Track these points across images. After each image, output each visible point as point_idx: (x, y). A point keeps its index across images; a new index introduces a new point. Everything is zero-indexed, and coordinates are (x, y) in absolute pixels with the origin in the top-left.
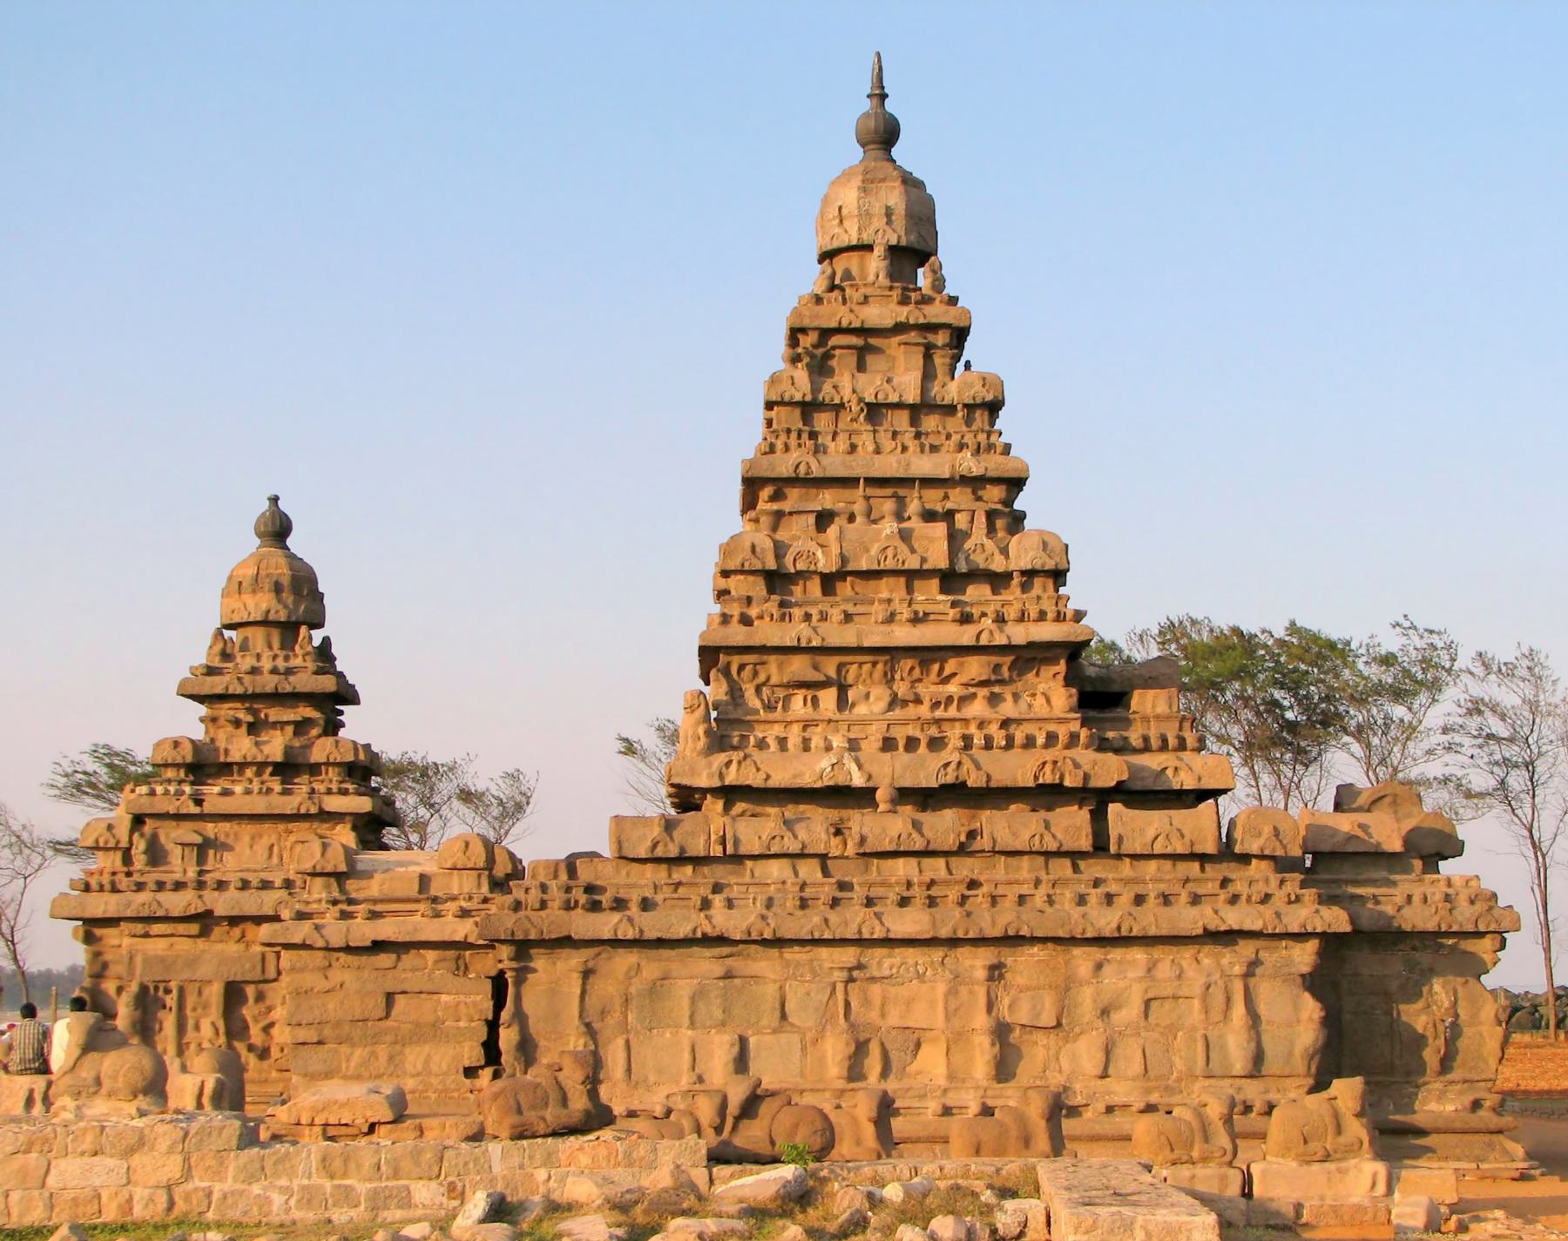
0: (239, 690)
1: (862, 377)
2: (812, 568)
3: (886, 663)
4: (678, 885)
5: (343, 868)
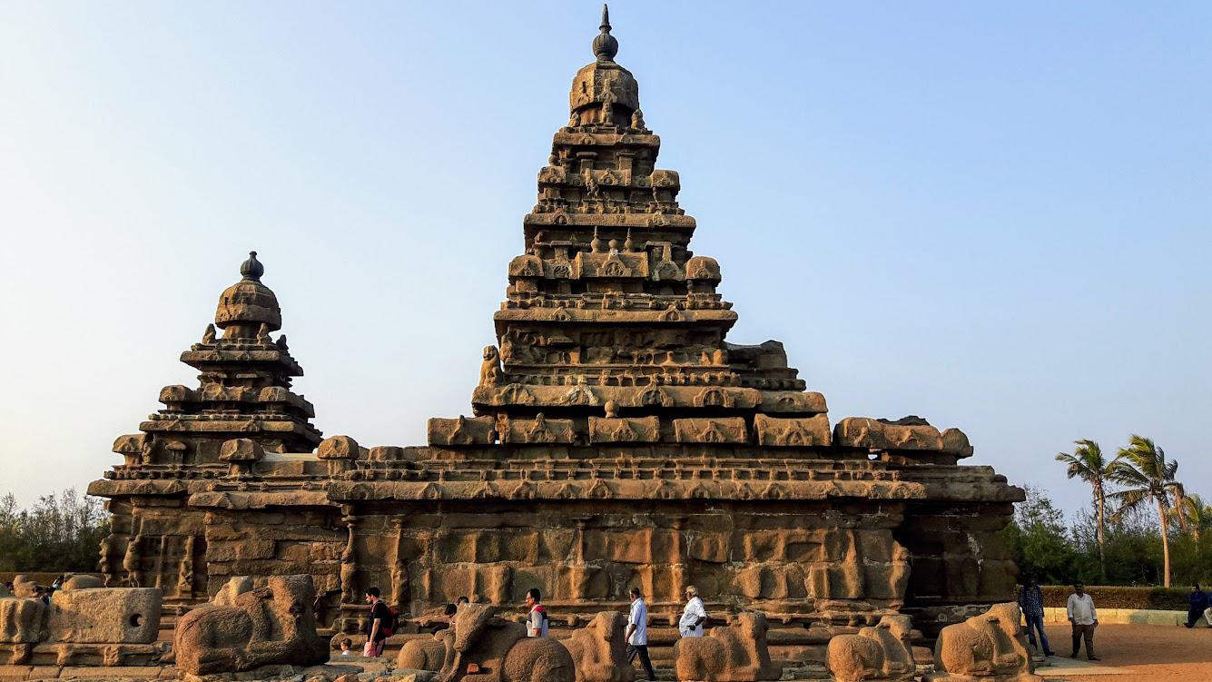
0: (219, 358)
2: (566, 276)
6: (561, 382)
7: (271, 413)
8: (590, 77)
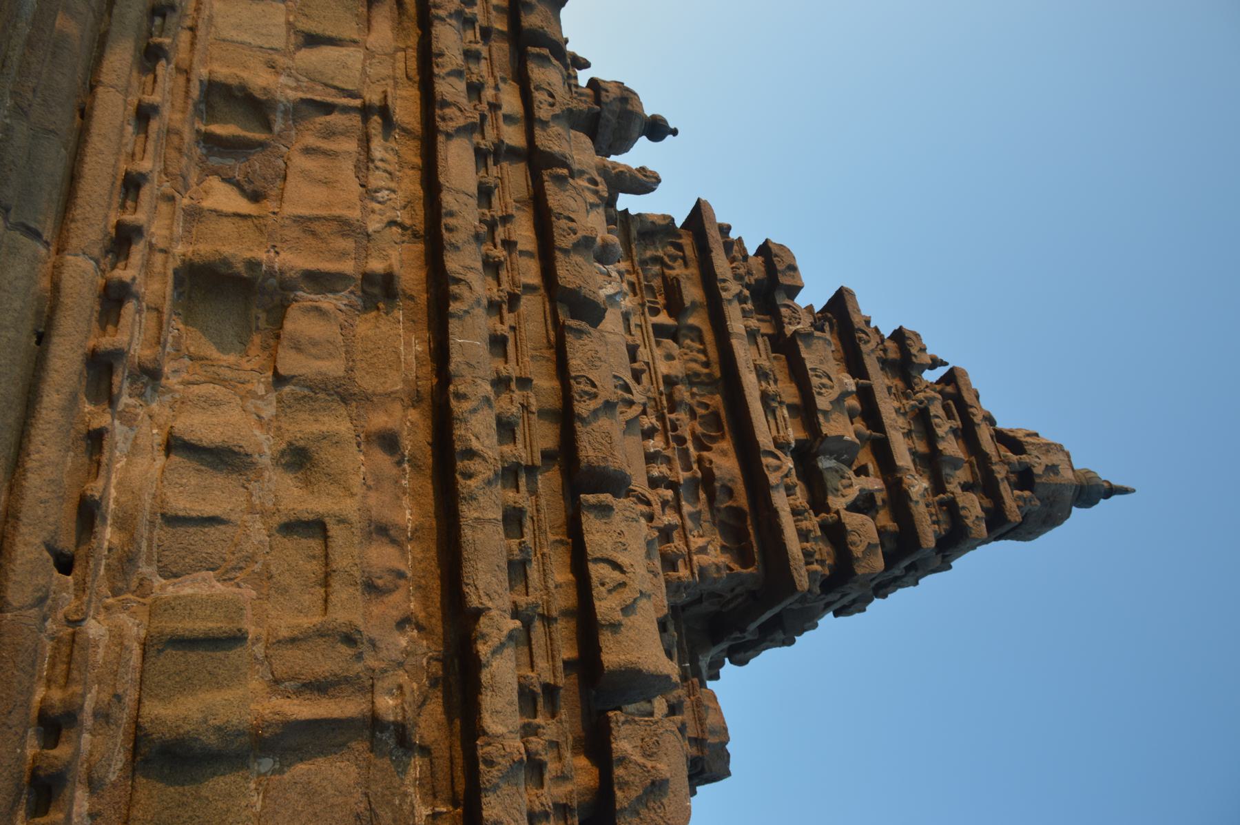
3: (709, 375)
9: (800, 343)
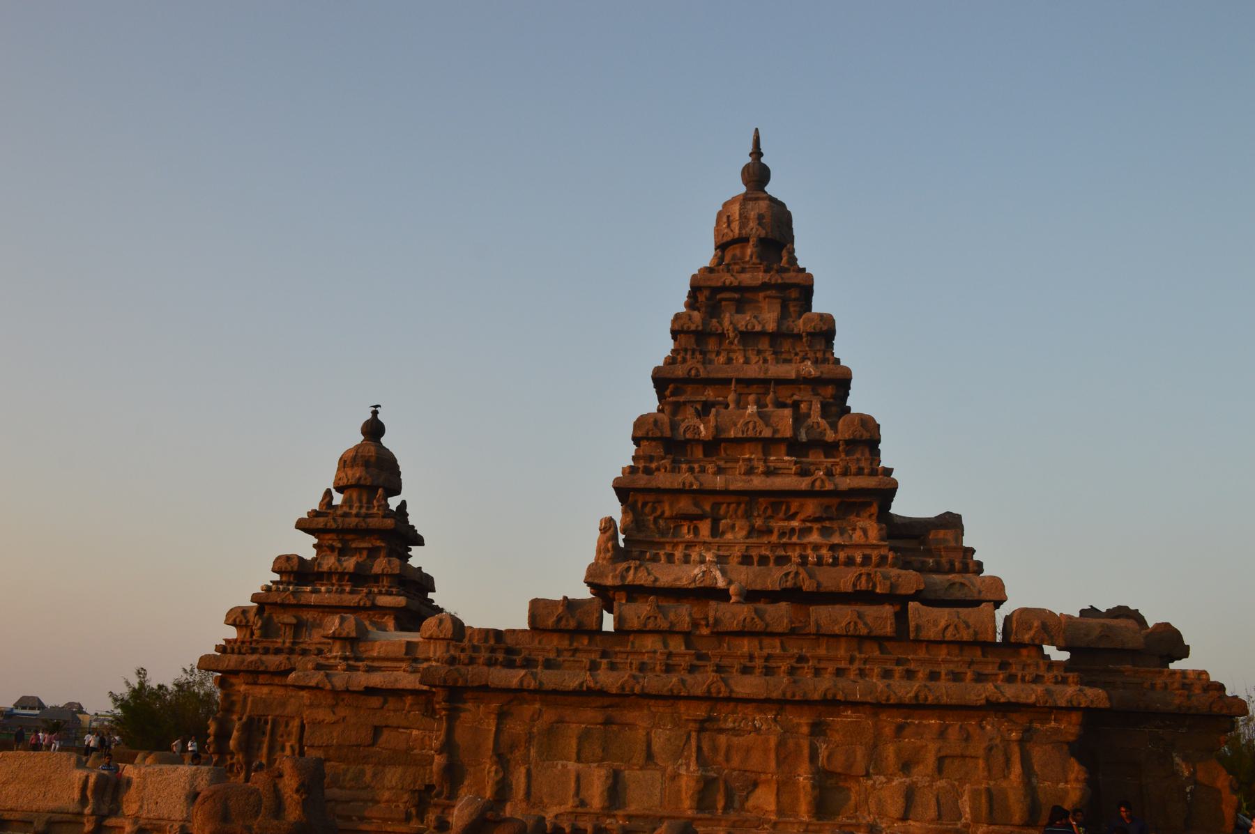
0: (334, 526)
1: (739, 316)
2: (697, 437)
4: (576, 650)
5: (353, 634)
6: (686, 559)
7: (383, 587)
8: (736, 208)
9: (722, 437)
